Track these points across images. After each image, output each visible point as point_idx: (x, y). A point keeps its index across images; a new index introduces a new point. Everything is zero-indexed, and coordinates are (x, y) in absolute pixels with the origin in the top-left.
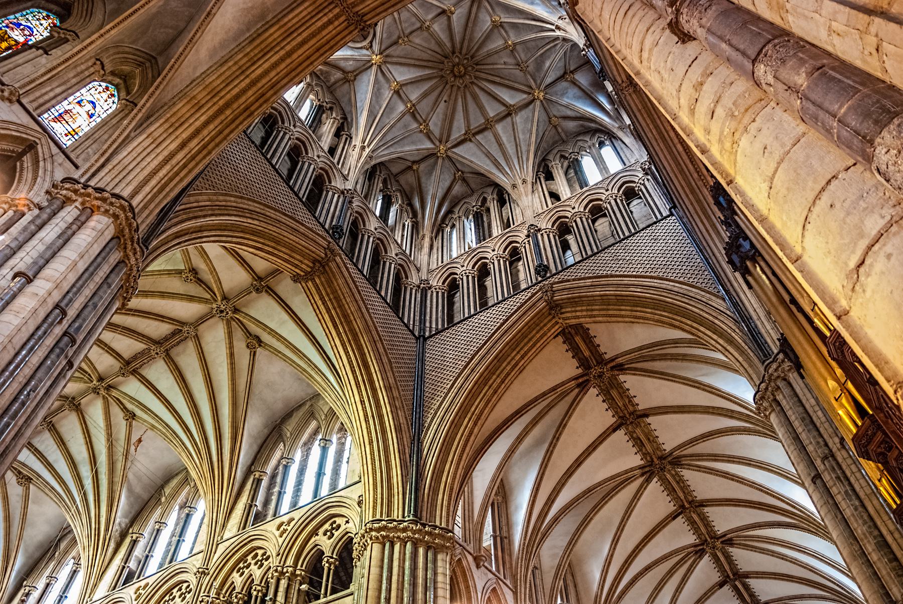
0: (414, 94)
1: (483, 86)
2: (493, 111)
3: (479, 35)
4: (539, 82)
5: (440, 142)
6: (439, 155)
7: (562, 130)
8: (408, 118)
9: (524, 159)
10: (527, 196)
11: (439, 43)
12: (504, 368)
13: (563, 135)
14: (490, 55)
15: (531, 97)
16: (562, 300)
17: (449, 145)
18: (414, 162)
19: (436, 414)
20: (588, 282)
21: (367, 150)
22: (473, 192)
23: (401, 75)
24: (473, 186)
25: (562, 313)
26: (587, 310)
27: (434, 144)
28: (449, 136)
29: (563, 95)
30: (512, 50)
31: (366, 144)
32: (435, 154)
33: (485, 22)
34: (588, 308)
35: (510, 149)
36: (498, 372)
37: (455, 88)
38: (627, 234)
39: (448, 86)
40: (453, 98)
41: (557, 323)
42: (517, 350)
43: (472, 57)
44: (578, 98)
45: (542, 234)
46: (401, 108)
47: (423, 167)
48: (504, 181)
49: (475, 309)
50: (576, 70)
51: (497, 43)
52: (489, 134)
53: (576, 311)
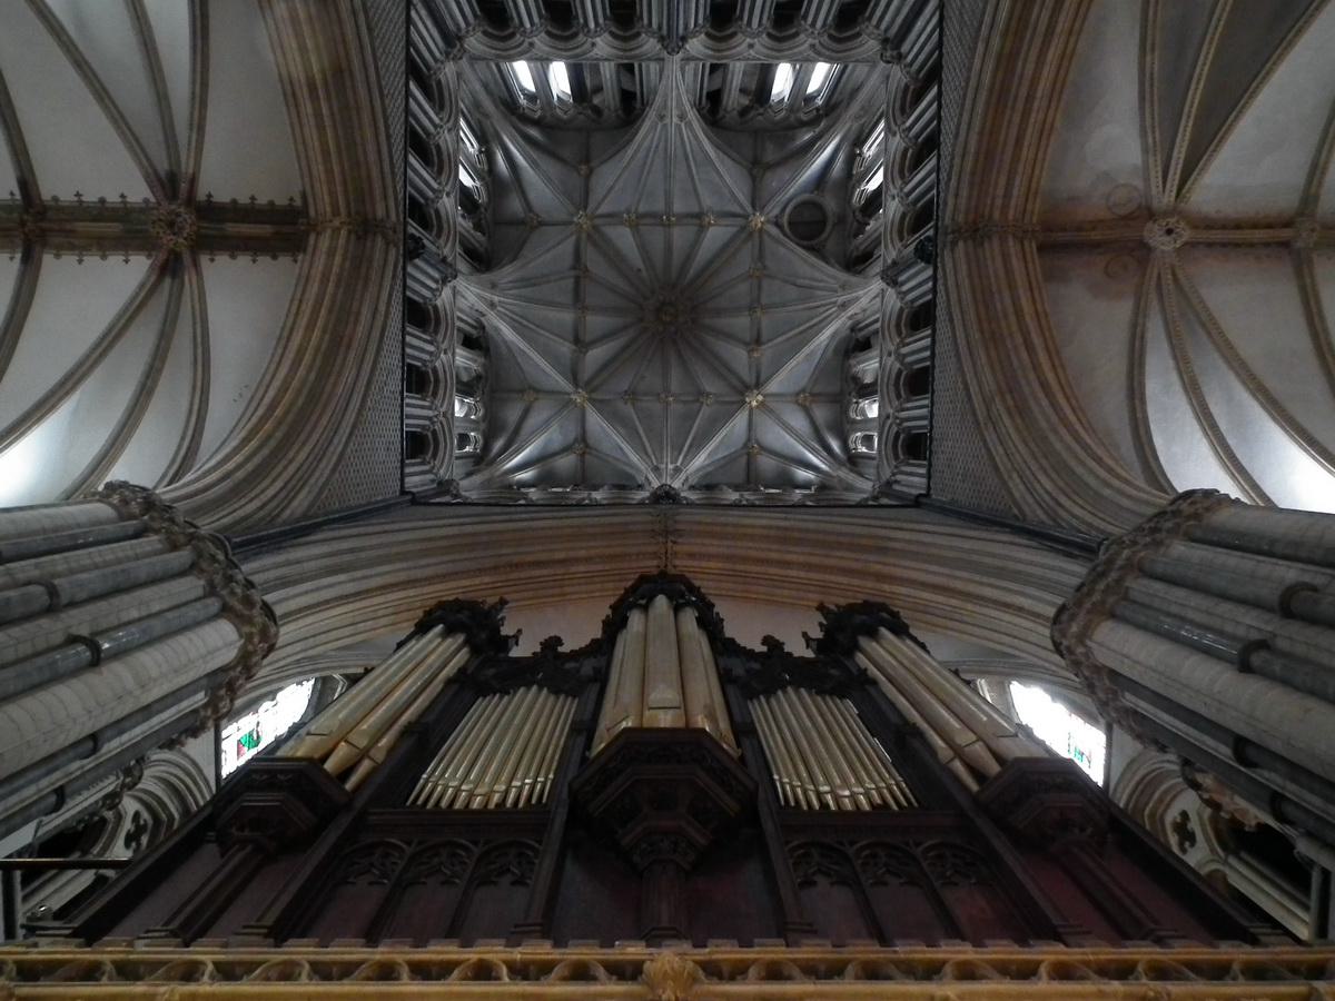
0: (680, 236)
5: (595, 227)
8: (660, 206)
11: (718, 312)
16: (373, 247)
18: (591, 171)
20: (382, 308)
23: (716, 235)
25: (350, 232)
27: (602, 216)
28: (595, 245)
32: (586, 208)
33: (711, 385)
38: (407, 410)
46: (678, 207)
50: (583, 461)
52: (568, 298)
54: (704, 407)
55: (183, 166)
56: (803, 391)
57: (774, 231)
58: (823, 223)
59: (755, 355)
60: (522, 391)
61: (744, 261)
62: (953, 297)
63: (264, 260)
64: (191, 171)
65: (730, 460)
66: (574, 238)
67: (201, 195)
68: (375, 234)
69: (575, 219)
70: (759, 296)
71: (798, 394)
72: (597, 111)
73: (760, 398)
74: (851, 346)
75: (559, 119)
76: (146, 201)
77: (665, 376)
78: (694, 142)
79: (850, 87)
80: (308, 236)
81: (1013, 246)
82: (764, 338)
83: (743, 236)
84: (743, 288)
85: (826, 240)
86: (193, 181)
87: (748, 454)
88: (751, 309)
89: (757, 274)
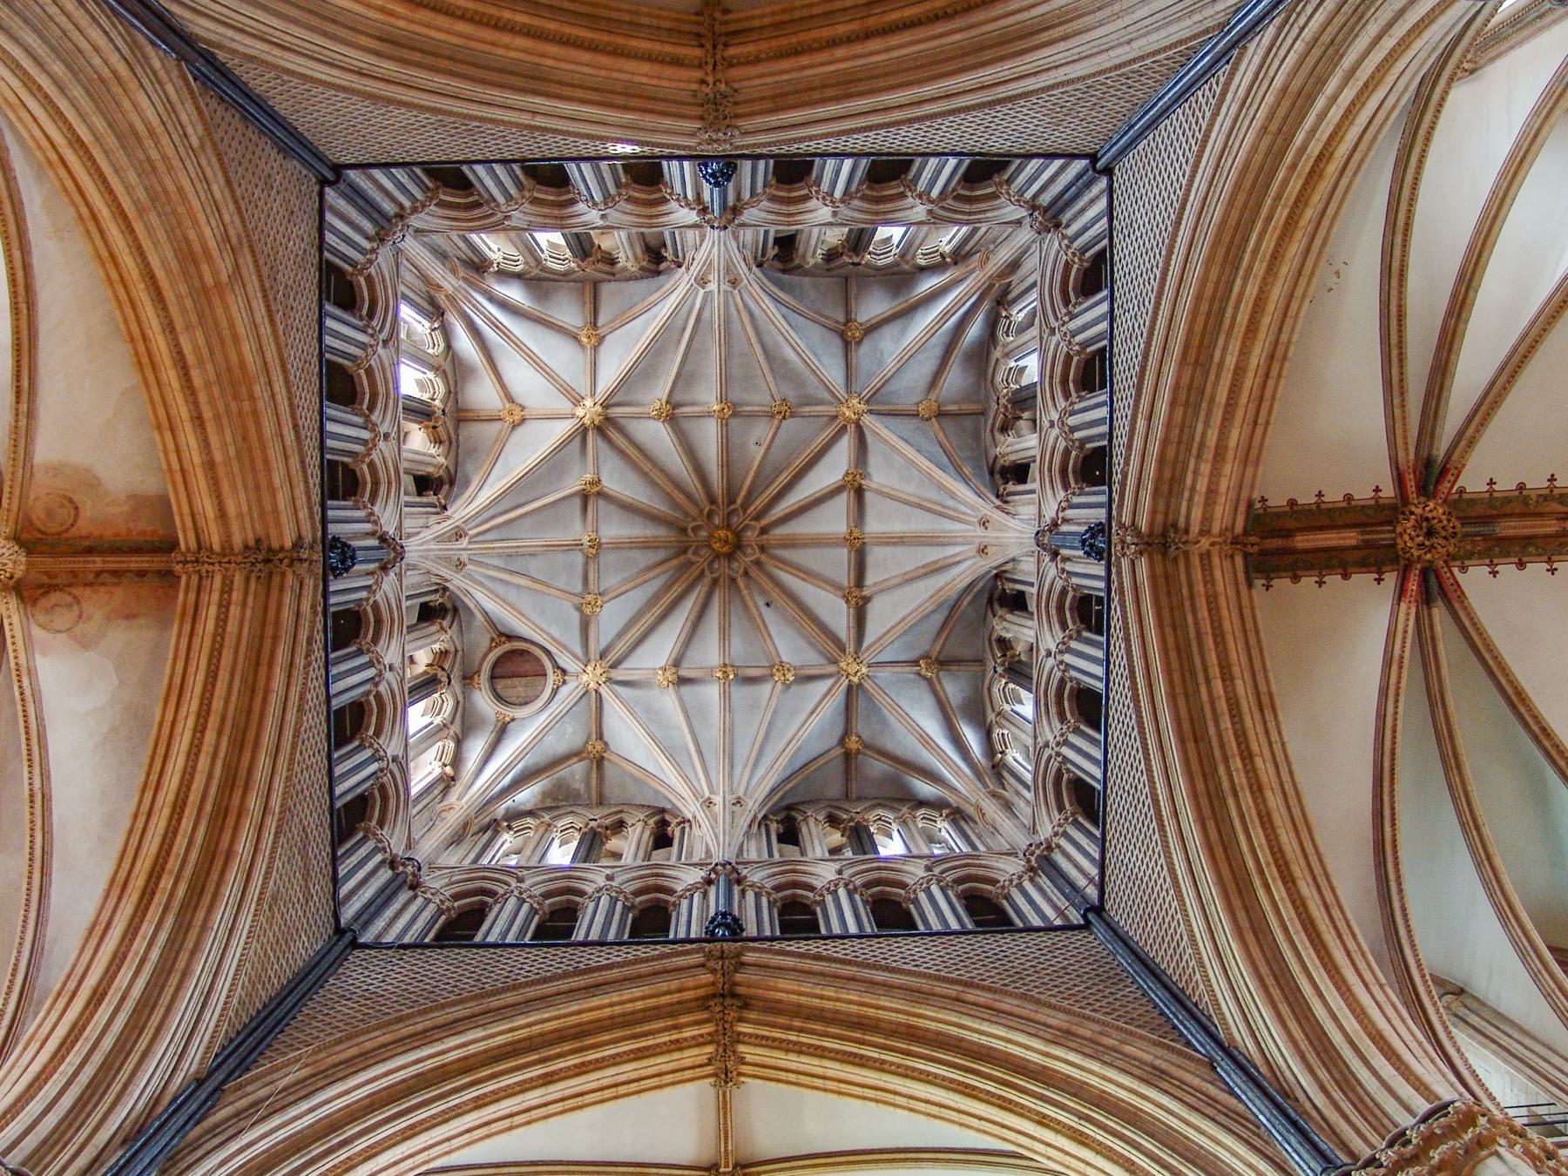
0: (709, 652)
1: (782, 514)
2: (834, 520)
3: (675, 461)
4: (827, 396)
5: (835, 662)
6: (856, 680)
7: (955, 403)
8: (738, 693)
9: (950, 503)
10: (1005, 528)
11: (646, 545)
12: (1220, 736)
13: (965, 407)
14: (727, 464)
15: (851, 428)
16: (1154, 512)
17: (851, 648)
18: (842, 742)
19: (1201, 964)
20: (1141, 424)
21: (718, 799)
22: (980, 661)
24: (968, 653)
25: (1187, 531)
26: (1199, 457)
29: (880, 364)
30: (733, 413)
31: (707, 794)
32: (850, 687)
33: (656, 436)
34: (1194, 451)
35: (921, 523)
36: (1217, 753)
37: (754, 572)
39: (741, 583)
40: (768, 585)
41: (1206, 557)
42: (1201, 680)
43: (713, 501)
44: (904, 331)
45: (1065, 521)
46: (711, 693)
47: (862, 728)
48: (968, 570)
49: (1094, 741)
51: (709, 437)
52: (875, 555)
53: (1193, 489)
54: (664, 397)
55: (1413, 610)
56: (515, 426)
57: (565, 661)
58: (493, 677)
59: (588, 477)
60: (941, 415)
61: (611, 619)
62: (294, 461)
63: (1307, 498)
64: (1403, 606)
65: (625, 317)
66: (865, 644)
67: (1391, 579)
68: (1151, 534)
69: (864, 670)
70: (586, 564)
71: (523, 420)
72: (833, 821)
73: (580, 412)
74: (446, 487)
75: (891, 808)
76: (1463, 569)
77: (726, 446)
78: (692, 776)
79: (465, 846)
80: (1245, 527)
81: (215, 540)
82: (577, 502)
83: (612, 656)
84: (611, 581)
85: (490, 649)
86: (1401, 593)
87: (595, 325)
88: (597, 545)
89: (589, 598)
